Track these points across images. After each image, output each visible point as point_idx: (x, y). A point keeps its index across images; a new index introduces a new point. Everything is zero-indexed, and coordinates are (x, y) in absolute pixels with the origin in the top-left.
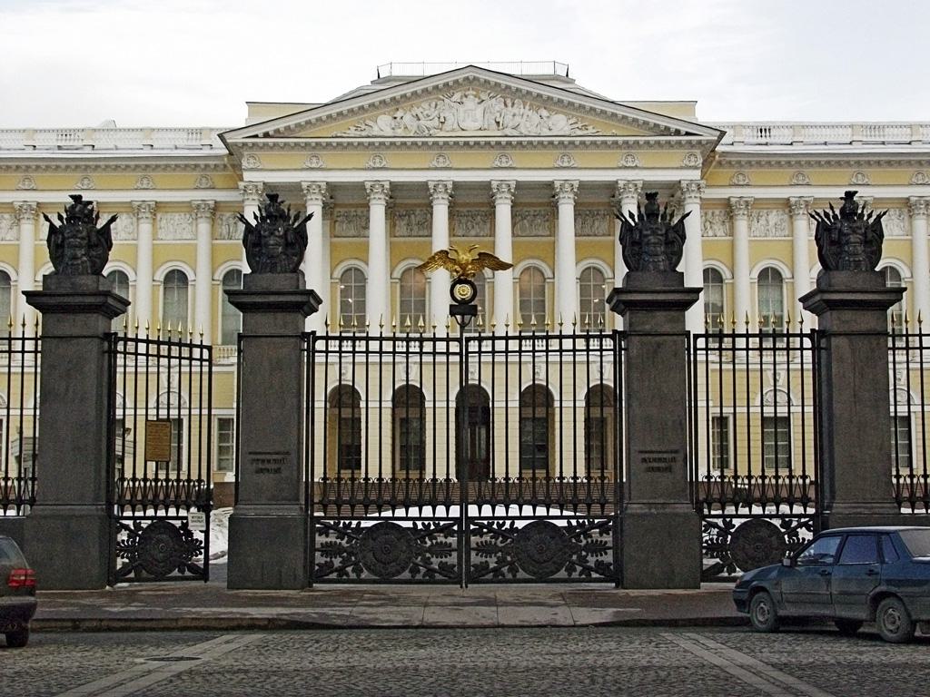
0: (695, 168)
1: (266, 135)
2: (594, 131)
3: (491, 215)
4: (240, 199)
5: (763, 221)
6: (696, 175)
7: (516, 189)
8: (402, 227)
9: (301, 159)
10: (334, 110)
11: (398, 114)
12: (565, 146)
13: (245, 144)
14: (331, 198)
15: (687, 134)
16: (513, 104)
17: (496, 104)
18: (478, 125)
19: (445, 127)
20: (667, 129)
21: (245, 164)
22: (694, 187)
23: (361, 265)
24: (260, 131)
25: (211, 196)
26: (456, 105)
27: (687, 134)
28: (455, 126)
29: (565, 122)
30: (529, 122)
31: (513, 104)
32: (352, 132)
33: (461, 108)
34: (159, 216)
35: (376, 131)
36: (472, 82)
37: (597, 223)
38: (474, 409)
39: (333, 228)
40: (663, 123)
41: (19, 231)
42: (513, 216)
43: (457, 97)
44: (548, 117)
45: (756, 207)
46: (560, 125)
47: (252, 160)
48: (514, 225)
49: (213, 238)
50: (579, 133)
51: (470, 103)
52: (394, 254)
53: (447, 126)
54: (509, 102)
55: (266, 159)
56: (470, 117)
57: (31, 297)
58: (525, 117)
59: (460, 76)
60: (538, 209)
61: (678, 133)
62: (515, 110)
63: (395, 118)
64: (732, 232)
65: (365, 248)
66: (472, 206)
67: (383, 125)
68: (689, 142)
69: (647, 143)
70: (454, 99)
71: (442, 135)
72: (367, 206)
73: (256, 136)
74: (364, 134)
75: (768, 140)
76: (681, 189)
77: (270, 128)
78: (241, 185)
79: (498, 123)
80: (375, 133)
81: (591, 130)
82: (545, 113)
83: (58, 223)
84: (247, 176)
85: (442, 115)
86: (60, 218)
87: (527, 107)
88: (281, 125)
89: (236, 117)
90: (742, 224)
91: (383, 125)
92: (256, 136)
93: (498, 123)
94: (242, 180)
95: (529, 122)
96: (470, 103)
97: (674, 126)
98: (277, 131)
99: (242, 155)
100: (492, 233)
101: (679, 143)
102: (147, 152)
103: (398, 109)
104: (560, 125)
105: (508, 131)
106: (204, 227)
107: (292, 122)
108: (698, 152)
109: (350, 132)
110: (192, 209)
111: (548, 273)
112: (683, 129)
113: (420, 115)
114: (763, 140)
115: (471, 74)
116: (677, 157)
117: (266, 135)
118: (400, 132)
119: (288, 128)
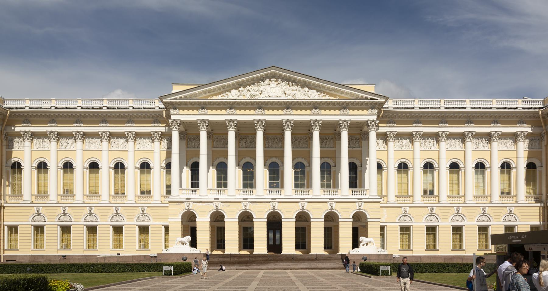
1: (181, 98)
2: (329, 98)
3: (282, 138)
6: (375, 118)
8: (243, 142)
11: (240, 89)
12: (315, 106)
13: (171, 103)
15: (371, 99)
18: (276, 95)
19: (261, 96)
21: (172, 111)
22: (373, 123)
27: (371, 99)
31: (292, 85)
35: (231, 97)
38: (274, 224)
42: (292, 139)
43: (267, 81)
45: (399, 136)
54: (290, 83)
60: (302, 136)
61: (367, 98)
62: (292, 88)
67: (233, 95)
68: (371, 103)
72: (227, 134)
73: (176, 99)
76: (367, 125)
78: (170, 121)
79: (285, 94)
80: (229, 98)
82: (307, 89)
84: (173, 117)
87: (299, 86)
92: (176, 99)
94: (171, 119)
96: (273, 84)
100: (283, 147)
104: (314, 95)
105: (290, 97)
113: (250, 90)
117: (181, 98)
118: (241, 97)
119: (191, 95)
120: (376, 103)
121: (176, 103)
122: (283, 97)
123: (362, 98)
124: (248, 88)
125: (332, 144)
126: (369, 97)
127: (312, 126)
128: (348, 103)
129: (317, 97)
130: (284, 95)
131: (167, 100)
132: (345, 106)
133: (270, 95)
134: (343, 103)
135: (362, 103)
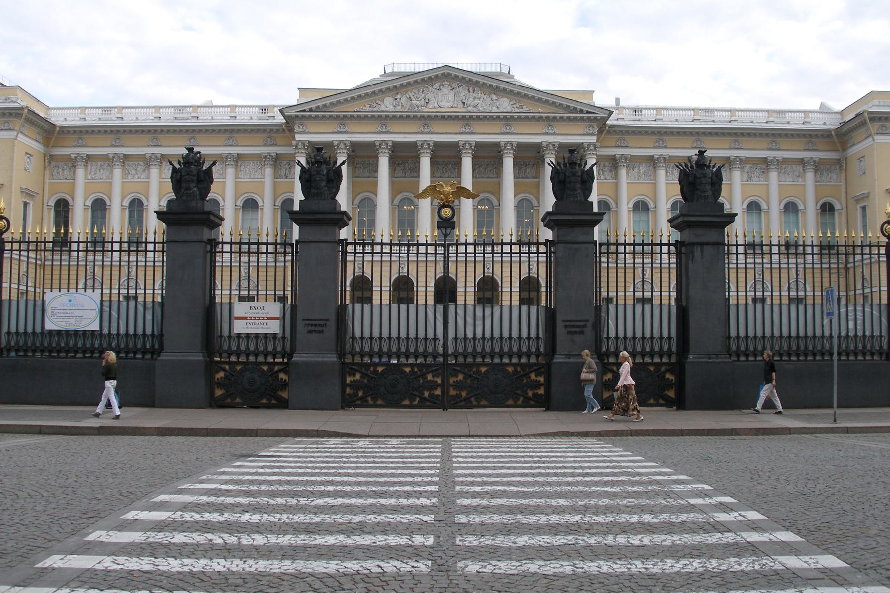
0: (593, 135)
1: (311, 110)
3: (458, 164)
4: (293, 152)
5: (636, 170)
9: (332, 126)
10: (355, 95)
11: (398, 97)
12: (507, 120)
13: (297, 116)
15: (588, 112)
17: (463, 92)
20: (575, 108)
21: (296, 129)
23: (372, 196)
24: (307, 108)
25: (274, 150)
27: (588, 112)
29: (507, 103)
30: (482, 103)
32: (367, 108)
33: (440, 94)
34: (239, 163)
35: (383, 108)
36: (447, 76)
37: (528, 170)
39: (353, 172)
40: (572, 105)
41: (149, 173)
42: (473, 164)
43: (437, 86)
45: (633, 162)
46: (505, 105)
47: (301, 127)
48: (473, 170)
49: (275, 178)
50: (517, 110)
51: (446, 90)
52: (394, 190)
53: (430, 106)
55: (312, 126)
56: (445, 100)
57: (160, 215)
59: (439, 73)
61: (581, 111)
62: (475, 95)
64: (616, 177)
65: (375, 185)
66: (446, 158)
68: (589, 118)
69: (562, 118)
70: (435, 87)
72: (377, 158)
73: (304, 111)
74: (375, 109)
75: (640, 117)
76: (584, 148)
77: (313, 106)
78: (294, 143)
81: (525, 109)
82: (494, 97)
83: (178, 166)
84: (298, 137)
86: (179, 162)
88: (320, 104)
89: (292, 99)
90: (623, 173)
91: (388, 105)
92: (304, 111)
94: (294, 139)
95: (482, 103)
96: (446, 90)
97: (579, 107)
98: (318, 107)
101: (582, 118)
102: (232, 122)
104: (505, 105)
105: (470, 109)
106: (269, 171)
107: (327, 102)
108: (595, 124)
109: (365, 108)
110: (260, 159)
111: (496, 202)
112: (586, 109)
114: (637, 117)
115: (446, 71)
116: (580, 128)
118: (399, 108)
119: (325, 106)
120: (596, 118)
121: (303, 116)
122: (460, 109)
124: (410, 94)
125: (534, 171)
127: (502, 150)
128: (555, 117)
129: (509, 109)
130: (462, 106)
131: (292, 113)
132: (550, 120)
133: (441, 104)
134: (548, 117)
135: (575, 118)
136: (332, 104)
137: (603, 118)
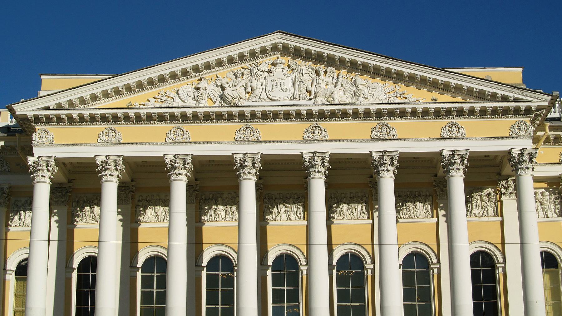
0: (524, 137)
1: (60, 107)
2: (414, 100)
6: (528, 144)
7: (330, 162)
11: (203, 84)
14: (132, 181)
15: (516, 100)
16: (325, 73)
17: (307, 69)
21: (35, 137)
22: (526, 157)
26: (264, 75)
27: (516, 100)
28: (264, 96)
31: (325, 73)
32: (153, 103)
33: (270, 78)
40: (489, 89)
44: (364, 85)
46: (378, 93)
58: (339, 86)
61: (505, 99)
63: (198, 88)
71: (248, 105)
73: (47, 108)
74: (164, 105)
78: (31, 160)
79: (310, 92)
81: (411, 98)
84: (37, 151)
85: (249, 85)
92: (47, 108)
93: (310, 92)
94: (32, 155)
99: (34, 131)
103: (201, 80)
108: (527, 120)
113: (226, 85)
120: (528, 111)
123: (494, 97)
126: (511, 95)
127: (376, 167)
133: (272, 95)
136: (94, 98)
137: (539, 109)
